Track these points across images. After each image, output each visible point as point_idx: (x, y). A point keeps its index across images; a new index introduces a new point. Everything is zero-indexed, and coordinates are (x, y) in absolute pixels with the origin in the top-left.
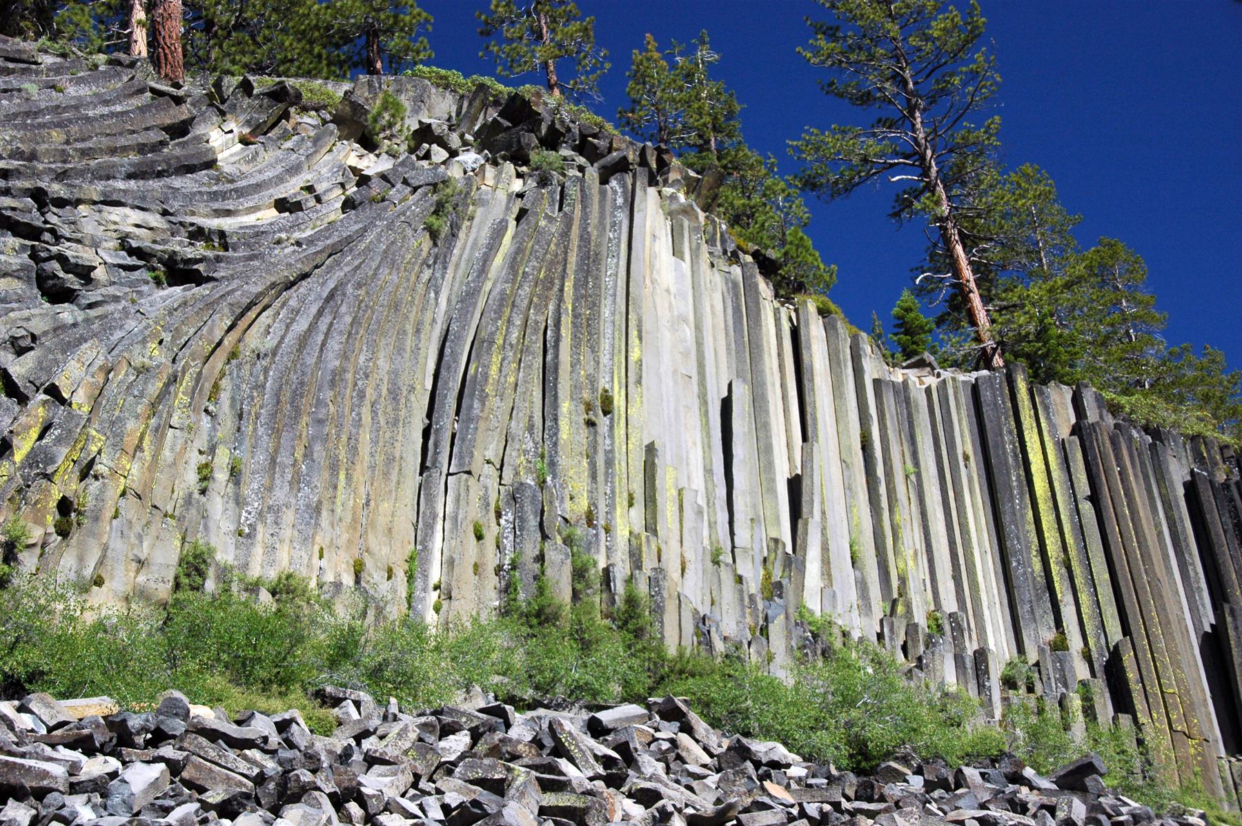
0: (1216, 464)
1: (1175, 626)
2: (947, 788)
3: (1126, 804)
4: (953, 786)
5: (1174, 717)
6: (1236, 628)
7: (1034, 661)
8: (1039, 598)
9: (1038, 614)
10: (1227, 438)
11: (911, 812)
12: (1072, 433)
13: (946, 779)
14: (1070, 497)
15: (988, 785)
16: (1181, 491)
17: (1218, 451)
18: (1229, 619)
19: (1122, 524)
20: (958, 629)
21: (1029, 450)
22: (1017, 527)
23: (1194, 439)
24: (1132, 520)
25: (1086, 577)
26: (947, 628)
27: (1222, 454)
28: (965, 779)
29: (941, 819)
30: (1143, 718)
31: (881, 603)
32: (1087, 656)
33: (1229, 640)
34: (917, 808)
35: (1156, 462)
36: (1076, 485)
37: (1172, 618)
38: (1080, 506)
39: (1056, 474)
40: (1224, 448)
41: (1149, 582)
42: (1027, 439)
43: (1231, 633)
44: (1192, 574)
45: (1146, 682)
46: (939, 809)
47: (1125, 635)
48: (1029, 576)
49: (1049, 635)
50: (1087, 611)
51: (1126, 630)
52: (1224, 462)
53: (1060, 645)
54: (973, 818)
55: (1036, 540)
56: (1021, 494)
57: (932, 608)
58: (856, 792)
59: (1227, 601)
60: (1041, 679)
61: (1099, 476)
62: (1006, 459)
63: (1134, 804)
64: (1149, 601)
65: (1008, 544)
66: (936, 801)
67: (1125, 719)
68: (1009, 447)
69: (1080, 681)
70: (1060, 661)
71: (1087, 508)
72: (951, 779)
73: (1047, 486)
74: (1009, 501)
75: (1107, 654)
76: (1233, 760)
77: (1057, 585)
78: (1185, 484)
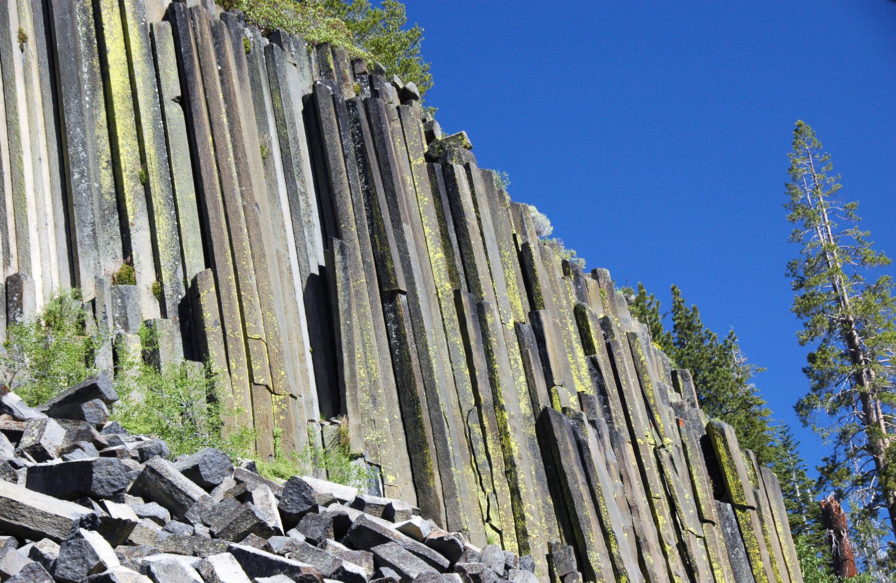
0: (345, 79)
1: (271, 261)
5: (256, 368)
6: (345, 268)
7: (87, 297)
8: (105, 220)
9: (101, 242)
10: (359, 51)
12: (164, 19)
14: (155, 97)
16: (298, 107)
17: (349, 64)
18: (338, 258)
19: (217, 134)
21: (107, 34)
22: (84, 132)
23: (320, 47)
24: (231, 131)
25: (167, 196)
27: (353, 69)
32: (160, 295)
33: (336, 282)
35: (271, 69)
36: (163, 83)
37: (270, 251)
38: (166, 109)
39: (141, 67)
40: (355, 62)
41: (244, 207)
42: (105, 19)
43: (339, 273)
44: (302, 205)
45: (226, 324)
47: (207, 266)
48: (95, 193)
49: (113, 265)
50: (163, 237)
51: (210, 262)
52: (355, 79)
53: (126, 278)
55: (107, 149)
56: (93, 90)
60: (95, 317)
61: (193, 73)
62: (76, 43)
65: (71, 151)
67: (195, 368)
68: (81, 30)
69: (146, 322)
70: (122, 297)
71: (175, 112)
73: (128, 81)
74: (76, 97)
76: (327, 424)
77: (129, 205)
78: (304, 99)
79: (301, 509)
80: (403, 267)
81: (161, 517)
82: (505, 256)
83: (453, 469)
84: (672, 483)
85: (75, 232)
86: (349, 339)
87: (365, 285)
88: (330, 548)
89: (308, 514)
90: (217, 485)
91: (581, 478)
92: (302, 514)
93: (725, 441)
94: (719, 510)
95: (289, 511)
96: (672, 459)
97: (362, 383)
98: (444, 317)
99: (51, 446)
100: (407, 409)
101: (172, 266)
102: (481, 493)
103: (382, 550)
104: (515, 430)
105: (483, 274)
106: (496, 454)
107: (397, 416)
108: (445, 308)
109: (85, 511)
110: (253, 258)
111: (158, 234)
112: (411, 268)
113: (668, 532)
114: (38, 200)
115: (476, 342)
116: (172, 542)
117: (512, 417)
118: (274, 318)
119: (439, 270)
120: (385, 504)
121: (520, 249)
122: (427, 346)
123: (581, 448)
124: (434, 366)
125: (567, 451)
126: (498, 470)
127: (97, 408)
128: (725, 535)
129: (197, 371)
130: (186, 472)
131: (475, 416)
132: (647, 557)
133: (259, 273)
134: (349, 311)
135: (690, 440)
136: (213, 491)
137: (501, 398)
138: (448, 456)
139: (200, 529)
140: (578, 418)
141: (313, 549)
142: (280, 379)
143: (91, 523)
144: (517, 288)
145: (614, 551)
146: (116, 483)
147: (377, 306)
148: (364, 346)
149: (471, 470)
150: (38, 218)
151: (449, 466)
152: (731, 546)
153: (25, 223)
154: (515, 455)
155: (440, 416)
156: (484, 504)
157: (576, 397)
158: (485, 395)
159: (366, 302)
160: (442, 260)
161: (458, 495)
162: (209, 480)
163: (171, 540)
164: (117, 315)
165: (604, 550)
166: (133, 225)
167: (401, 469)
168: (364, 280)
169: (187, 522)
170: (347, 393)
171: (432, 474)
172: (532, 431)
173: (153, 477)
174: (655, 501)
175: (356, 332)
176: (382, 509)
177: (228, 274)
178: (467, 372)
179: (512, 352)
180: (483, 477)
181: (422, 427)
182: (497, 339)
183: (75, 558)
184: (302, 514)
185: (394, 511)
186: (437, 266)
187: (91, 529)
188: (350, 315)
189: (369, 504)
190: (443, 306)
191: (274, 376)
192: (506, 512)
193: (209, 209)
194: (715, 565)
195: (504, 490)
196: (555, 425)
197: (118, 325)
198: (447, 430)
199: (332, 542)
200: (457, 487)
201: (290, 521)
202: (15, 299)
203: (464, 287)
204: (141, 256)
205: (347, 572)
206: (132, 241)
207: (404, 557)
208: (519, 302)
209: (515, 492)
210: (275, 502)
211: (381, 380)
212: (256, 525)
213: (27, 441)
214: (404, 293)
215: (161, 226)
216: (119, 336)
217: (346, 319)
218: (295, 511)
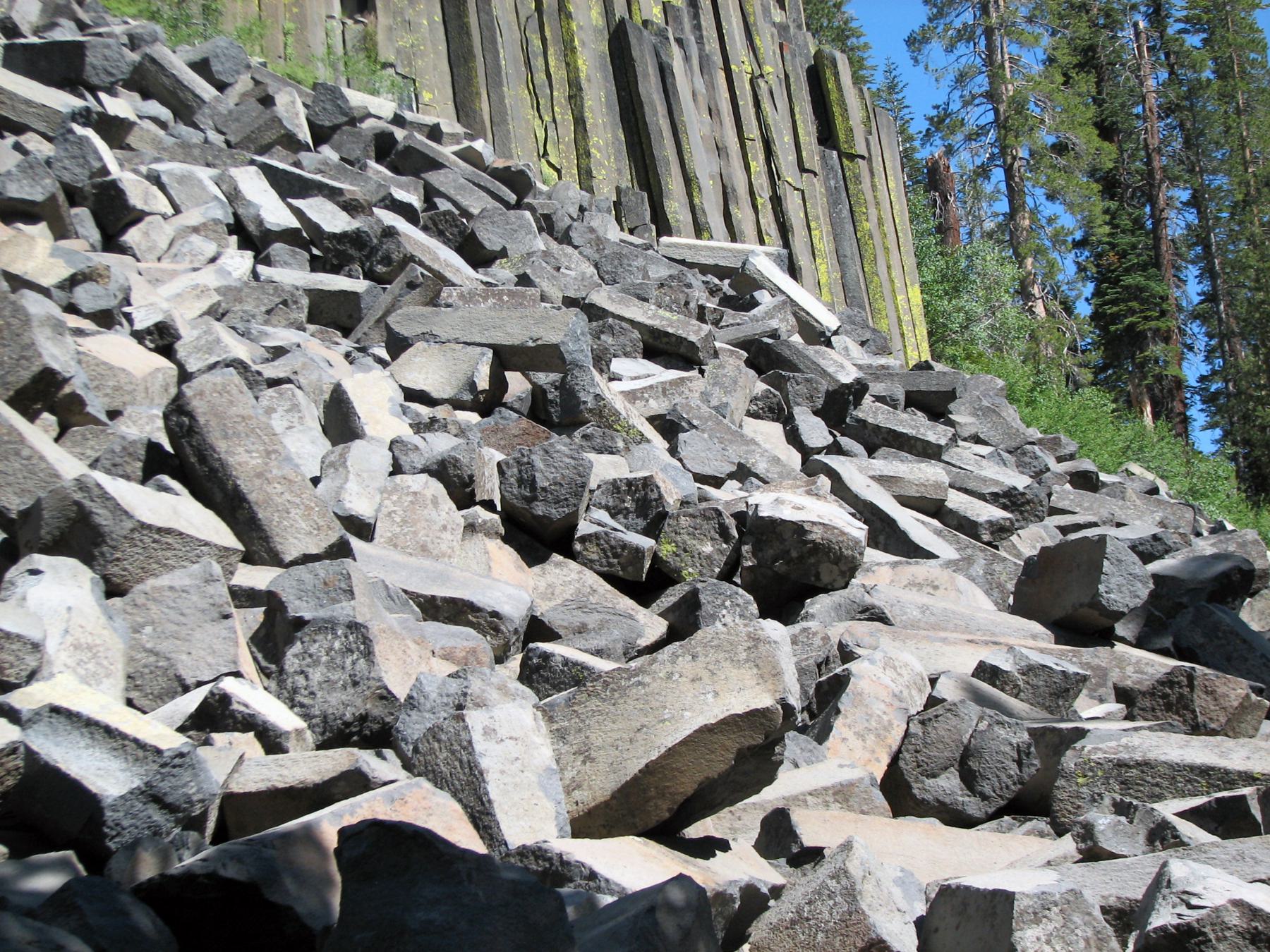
76: (349, 22)
79: (336, 122)
81: (163, 118)
83: (505, 89)
84: (770, 121)
91: (661, 109)
92: (335, 128)
93: (836, 74)
94: (823, 157)
96: (771, 93)
100: (451, 11)
102: (537, 121)
103: (434, 178)
104: (583, 44)
106: (559, 74)
107: (438, 18)
109: (77, 103)
113: (762, 182)
117: (580, 27)
123: (664, 72)
125: (646, 75)
126: (560, 94)
128: (828, 189)
131: (534, 23)
132: (734, 210)
135: (795, 69)
138: (500, 72)
139: (213, 136)
140: (662, 34)
143: (84, 117)
145: (696, 201)
146: (114, 71)
151: (500, 84)
152: (833, 203)
154: (583, 76)
155: (492, 21)
156: (541, 134)
157: (660, 7)
161: (510, 122)
165: (685, 200)
171: (478, 94)
172: (604, 47)
173: (153, 68)
174: (748, 143)
181: (468, 34)
183: (74, 157)
184: (335, 128)
189: (411, 123)
194: (813, 225)
195: (565, 117)
196: (633, 41)
198: (499, 39)
199: (372, 163)
201: (321, 135)
209: (580, 122)
210: (302, 112)
212: (283, 136)
218: (327, 124)
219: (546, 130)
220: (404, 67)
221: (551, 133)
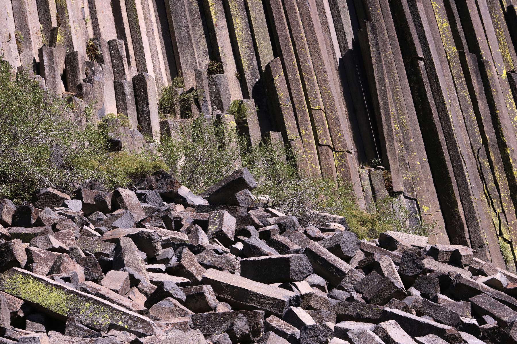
2: (105, 211)
3: (273, 215)
4: (110, 207)
5: (320, 132)
6: (377, 45)
11: (68, 234)
13: (104, 202)
15: (145, 205)
18: (370, 37)
20: (116, 56)
26: (107, 57)
28: (122, 200)
29: (98, 240)
30: (292, 134)
31: (40, 33)
34: (74, 229)
43: (373, 49)
45: (295, 100)
46: (96, 230)
47: (275, 56)
50: (240, 34)
51: (277, 52)
54: (128, 236)
57: (92, 36)
58: (14, 218)
59: (370, 19)
63: (281, 214)
64: (298, 22)
66: (94, 223)
67: (275, 136)
72: (108, 201)
75: (259, 76)
79: (415, 273)
80: (419, 38)
81: (322, 284)
82: (495, 18)
83: (472, 197)
85: (174, 34)
86: (384, 102)
87: (392, 55)
88: (441, 300)
89: (420, 276)
90: (352, 257)
95: (407, 274)
97: (397, 135)
98: (453, 75)
99: (229, 231)
101: (248, 56)
102: (493, 214)
103: (477, 300)
105: (480, 36)
107: (425, 159)
108: (453, 67)
110: (308, 44)
111: (236, 32)
112: (426, 39)
114: (145, 11)
115: (480, 93)
116: (341, 307)
117: (512, 151)
118: (329, 92)
119: (446, 36)
120: (453, 250)
121: (506, 10)
122: (443, 101)
124: (450, 116)
127: (246, 196)
129: (277, 138)
130: (330, 249)
131: (483, 151)
133: (314, 57)
134: (382, 80)
136: (351, 262)
137: (503, 137)
138: (467, 187)
141: (433, 305)
142: (338, 140)
144: (506, 44)
146: (305, 271)
147: (402, 71)
148: (396, 105)
149: (484, 196)
150: (146, 26)
151: (469, 195)
153: (138, 31)
156: (496, 221)
158: (491, 135)
159: (395, 70)
160: (447, 28)
161: (478, 218)
162: (347, 254)
163: (340, 305)
164: (213, 99)
166: (216, 26)
167: (432, 201)
168: (391, 52)
169: (343, 289)
170: (387, 145)
171: (456, 203)
175: (389, 94)
176: (450, 254)
177: (293, 60)
178: (475, 118)
179: (507, 98)
180: (494, 201)
182: (497, 89)
183: (312, 337)
184: (416, 276)
185: (460, 255)
186: (445, 34)
187: (297, 306)
188: (384, 82)
189: (442, 252)
190: (452, 66)
191: (333, 138)
192: (513, 227)
193: (273, 9)
197: (215, 107)
198: (464, 167)
199: (442, 297)
200: (476, 212)
201: (408, 282)
202: (142, 93)
203: (466, 47)
204: (225, 50)
205: (466, 323)
206: (217, 38)
207: (493, 304)
208: (509, 55)
211: (411, 132)
212: (396, 291)
213: (212, 228)
214: (421, 59)
215: (237, 25)
216: (218, 116)
217: (381, 86)
218: (411, 274)
219: (499, 218)
220: (409, 192)
221: (503, 220)
